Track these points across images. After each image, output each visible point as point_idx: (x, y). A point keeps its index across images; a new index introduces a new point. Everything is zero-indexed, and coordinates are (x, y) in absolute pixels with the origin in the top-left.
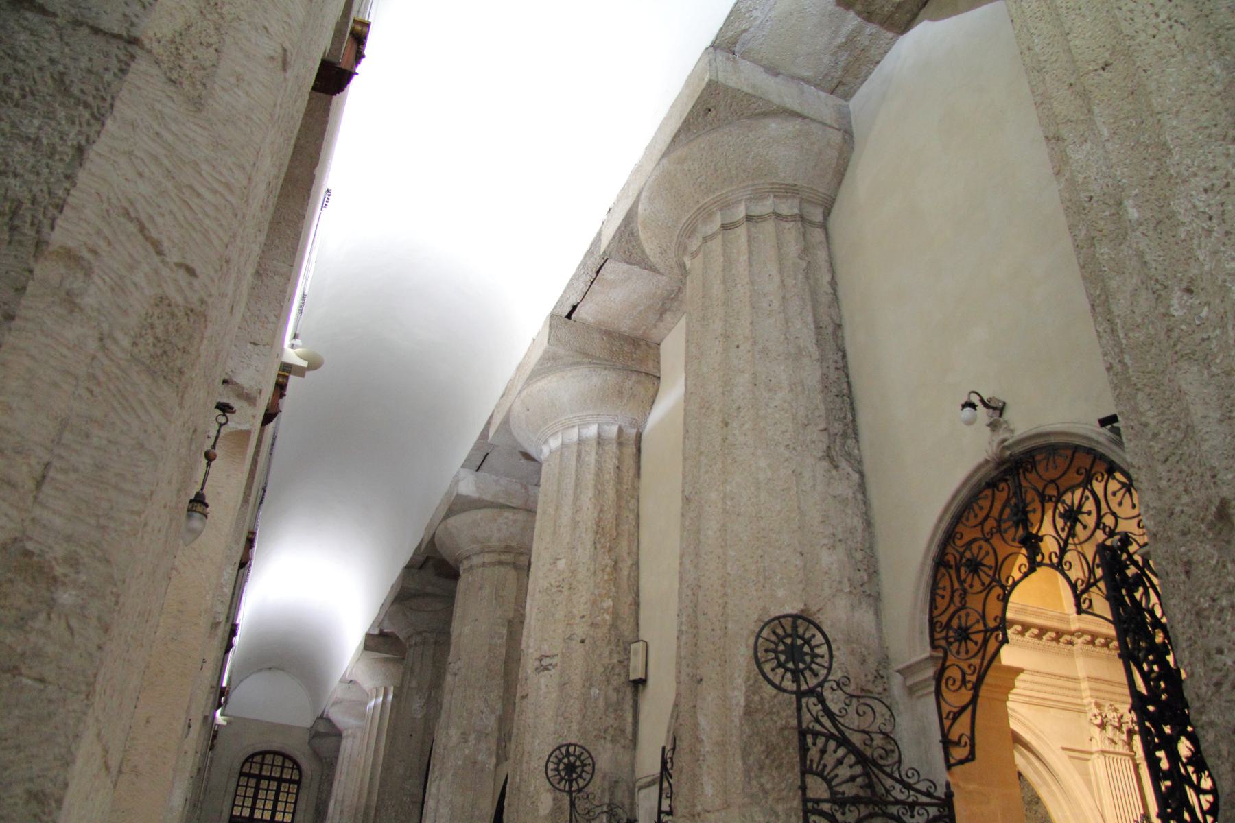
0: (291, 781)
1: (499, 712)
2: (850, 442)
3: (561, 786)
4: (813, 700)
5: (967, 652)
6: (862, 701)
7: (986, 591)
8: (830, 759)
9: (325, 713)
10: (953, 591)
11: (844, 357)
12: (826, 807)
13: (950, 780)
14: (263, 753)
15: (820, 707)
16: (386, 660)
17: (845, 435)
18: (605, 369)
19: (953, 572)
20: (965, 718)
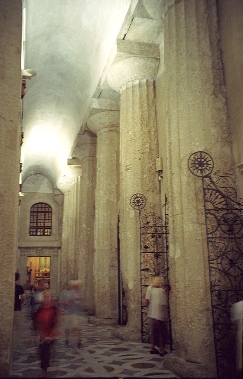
0: (48, 212)
3: (136, 208)
4: (208, 178)
6: (225, 178)
8: (213, 197)
12: (212, 211)
17: (220, 84)
18: (139, 58)
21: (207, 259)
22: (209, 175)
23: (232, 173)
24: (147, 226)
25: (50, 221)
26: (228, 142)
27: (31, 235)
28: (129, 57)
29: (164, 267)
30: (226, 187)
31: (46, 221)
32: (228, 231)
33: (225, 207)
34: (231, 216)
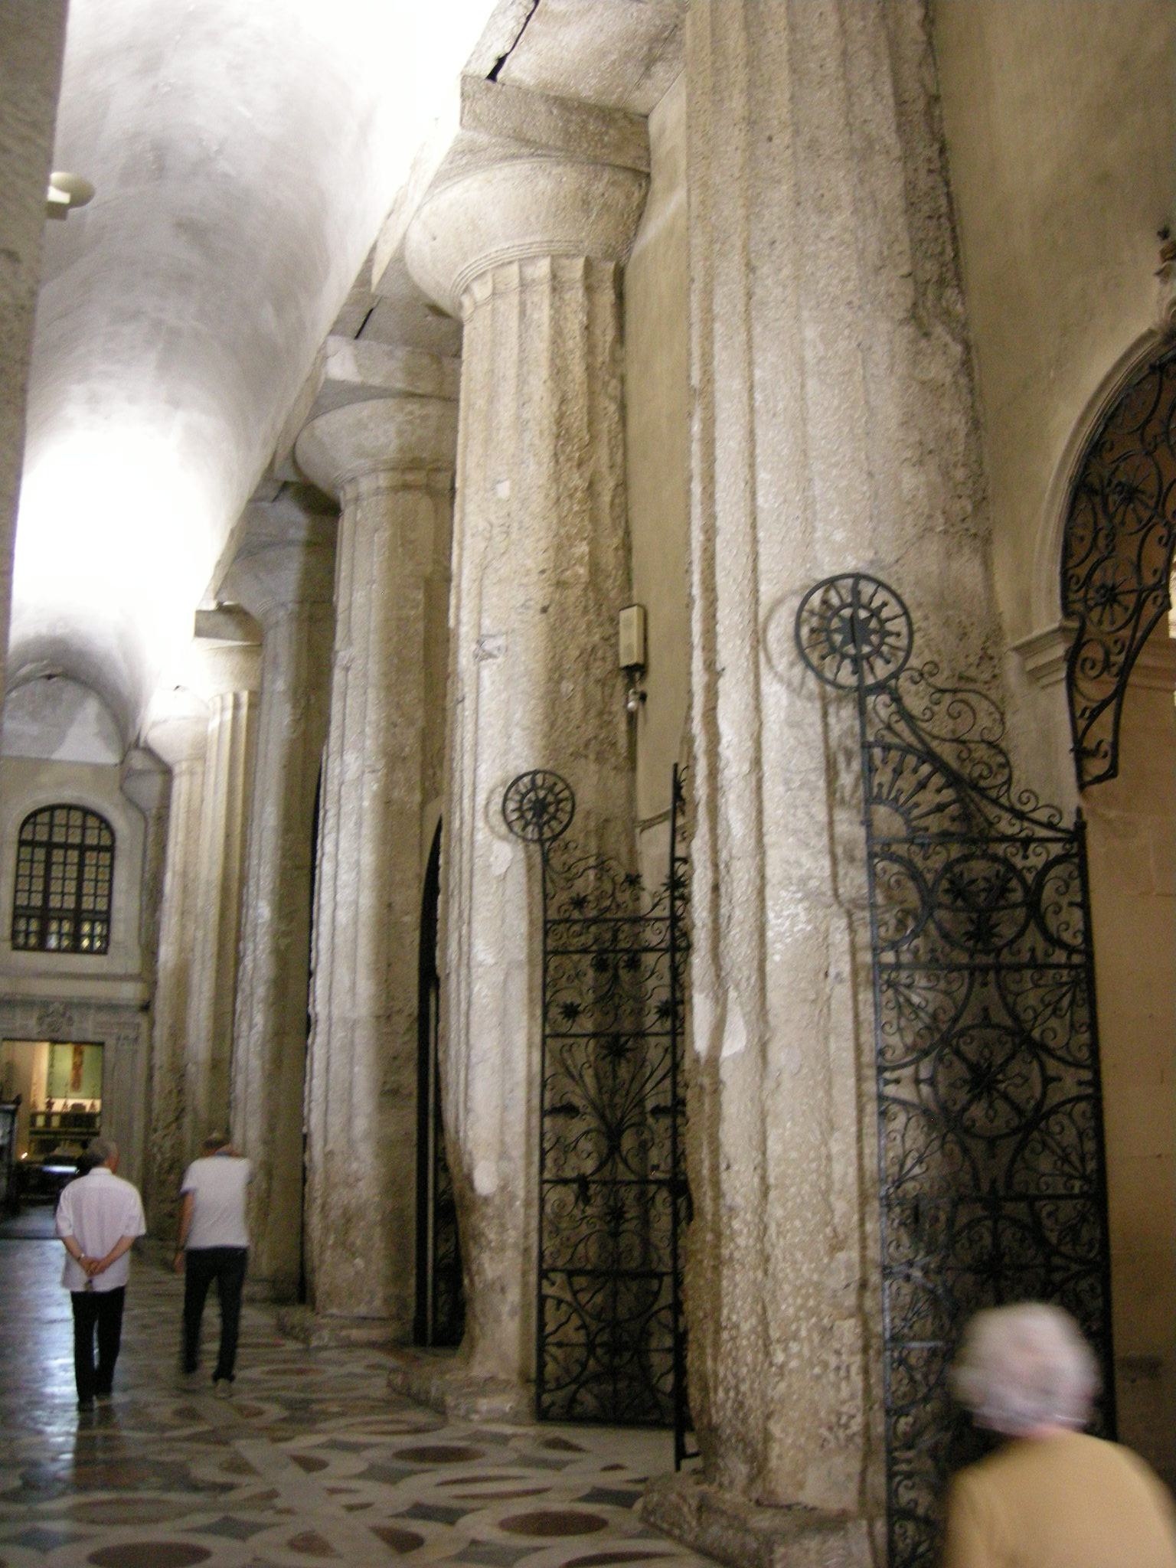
0: (98, 848)
1: (420, 723)
2: (950, 293)
4: (884, 698)
5: (1113, 623)
6: (960, 696)
7: (1142, 533)
8: (906, 783)
9: (142, 740)
10: (1096, 532)
11: (942, 151)
12: (901, 849)
13: (1084, 805)
14: (52, 809)
15: (893, 707)
16: (231, 650)
17: (941, 282)
19: (1097, 500)
20: (1108, 715)
21: (869, 1057)
22: (893, 682)
23: (986, 676)
24: (576, 915)
25: (103, 888)
26: (975, 535)
28: (514, 157)
29: (642, 1101)
30: (965, 737)
31: (88, 888)
32: (970, 936)
33: (954, 828)
34: (980, 868)
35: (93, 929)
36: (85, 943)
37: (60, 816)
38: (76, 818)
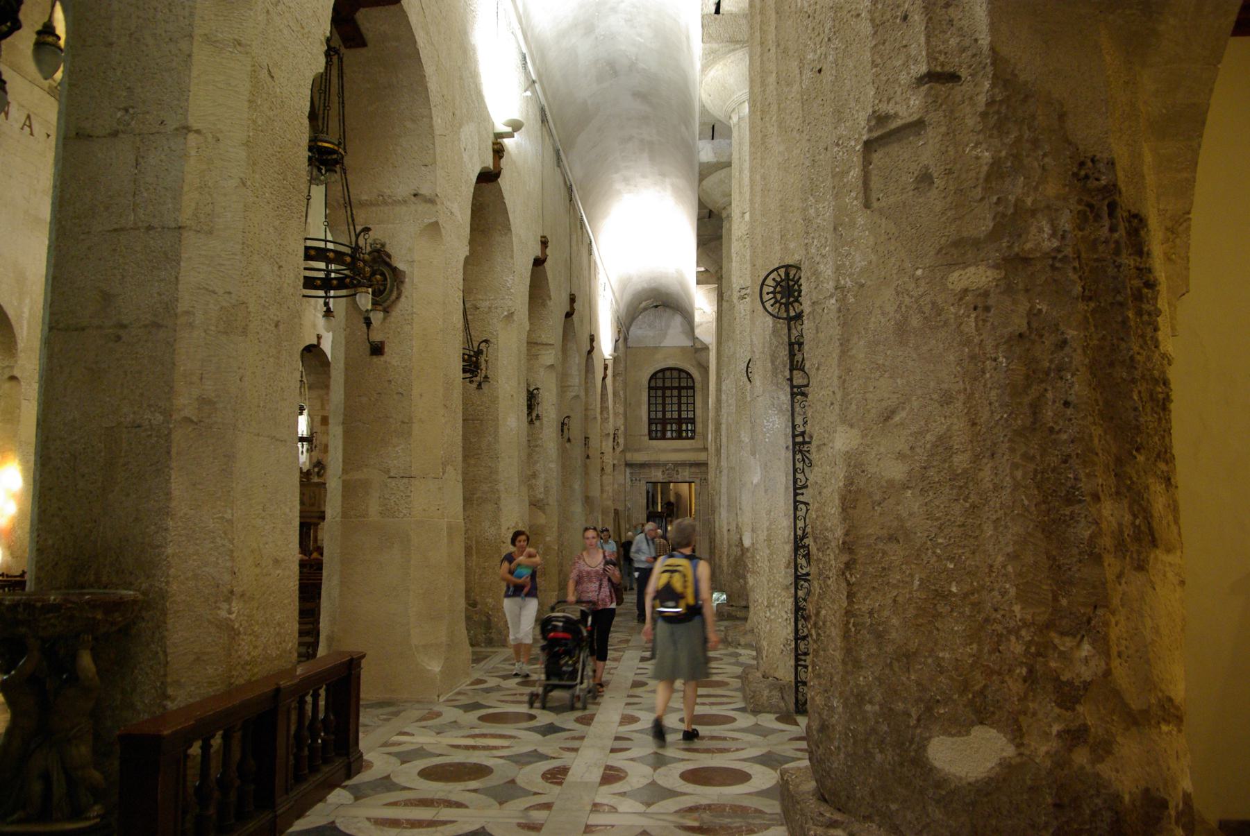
0: (687, 388)
14: (663, 370)
25: (691, 407)
27: (650, 439)
31: (684, 407)
35: (687, 427)
36: (684, 434)
37: (668, 374)
38: (675, 374)
